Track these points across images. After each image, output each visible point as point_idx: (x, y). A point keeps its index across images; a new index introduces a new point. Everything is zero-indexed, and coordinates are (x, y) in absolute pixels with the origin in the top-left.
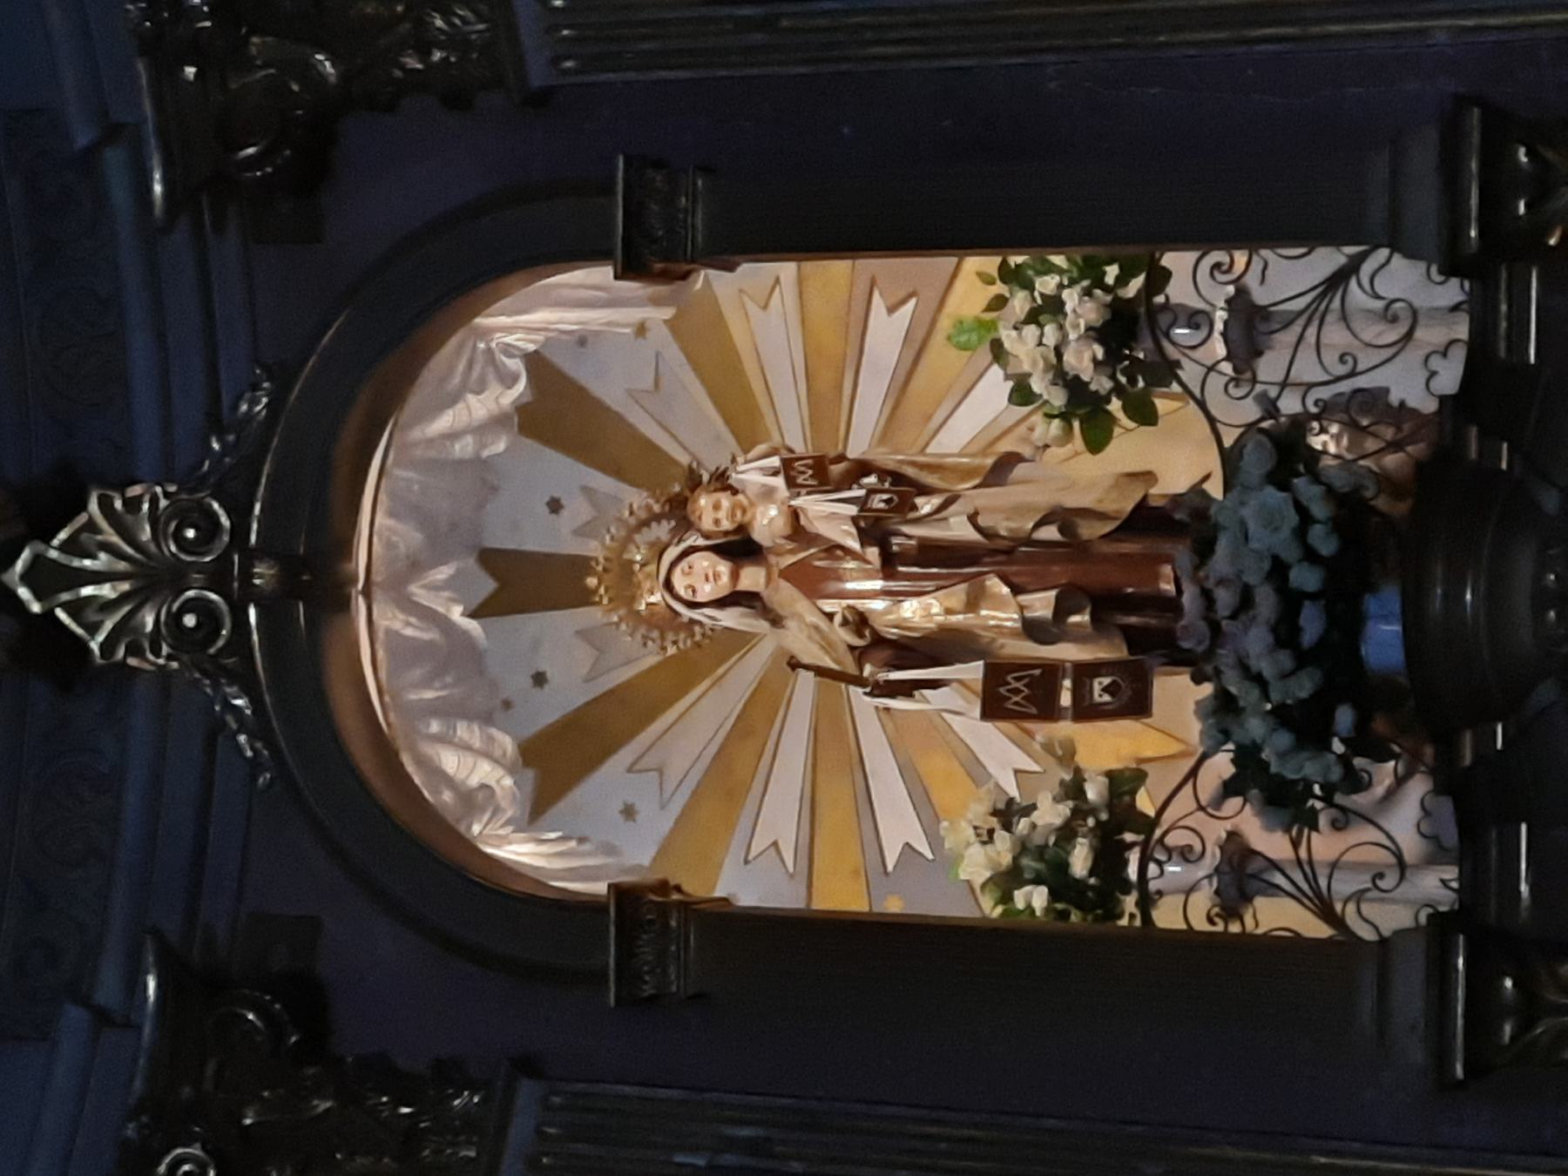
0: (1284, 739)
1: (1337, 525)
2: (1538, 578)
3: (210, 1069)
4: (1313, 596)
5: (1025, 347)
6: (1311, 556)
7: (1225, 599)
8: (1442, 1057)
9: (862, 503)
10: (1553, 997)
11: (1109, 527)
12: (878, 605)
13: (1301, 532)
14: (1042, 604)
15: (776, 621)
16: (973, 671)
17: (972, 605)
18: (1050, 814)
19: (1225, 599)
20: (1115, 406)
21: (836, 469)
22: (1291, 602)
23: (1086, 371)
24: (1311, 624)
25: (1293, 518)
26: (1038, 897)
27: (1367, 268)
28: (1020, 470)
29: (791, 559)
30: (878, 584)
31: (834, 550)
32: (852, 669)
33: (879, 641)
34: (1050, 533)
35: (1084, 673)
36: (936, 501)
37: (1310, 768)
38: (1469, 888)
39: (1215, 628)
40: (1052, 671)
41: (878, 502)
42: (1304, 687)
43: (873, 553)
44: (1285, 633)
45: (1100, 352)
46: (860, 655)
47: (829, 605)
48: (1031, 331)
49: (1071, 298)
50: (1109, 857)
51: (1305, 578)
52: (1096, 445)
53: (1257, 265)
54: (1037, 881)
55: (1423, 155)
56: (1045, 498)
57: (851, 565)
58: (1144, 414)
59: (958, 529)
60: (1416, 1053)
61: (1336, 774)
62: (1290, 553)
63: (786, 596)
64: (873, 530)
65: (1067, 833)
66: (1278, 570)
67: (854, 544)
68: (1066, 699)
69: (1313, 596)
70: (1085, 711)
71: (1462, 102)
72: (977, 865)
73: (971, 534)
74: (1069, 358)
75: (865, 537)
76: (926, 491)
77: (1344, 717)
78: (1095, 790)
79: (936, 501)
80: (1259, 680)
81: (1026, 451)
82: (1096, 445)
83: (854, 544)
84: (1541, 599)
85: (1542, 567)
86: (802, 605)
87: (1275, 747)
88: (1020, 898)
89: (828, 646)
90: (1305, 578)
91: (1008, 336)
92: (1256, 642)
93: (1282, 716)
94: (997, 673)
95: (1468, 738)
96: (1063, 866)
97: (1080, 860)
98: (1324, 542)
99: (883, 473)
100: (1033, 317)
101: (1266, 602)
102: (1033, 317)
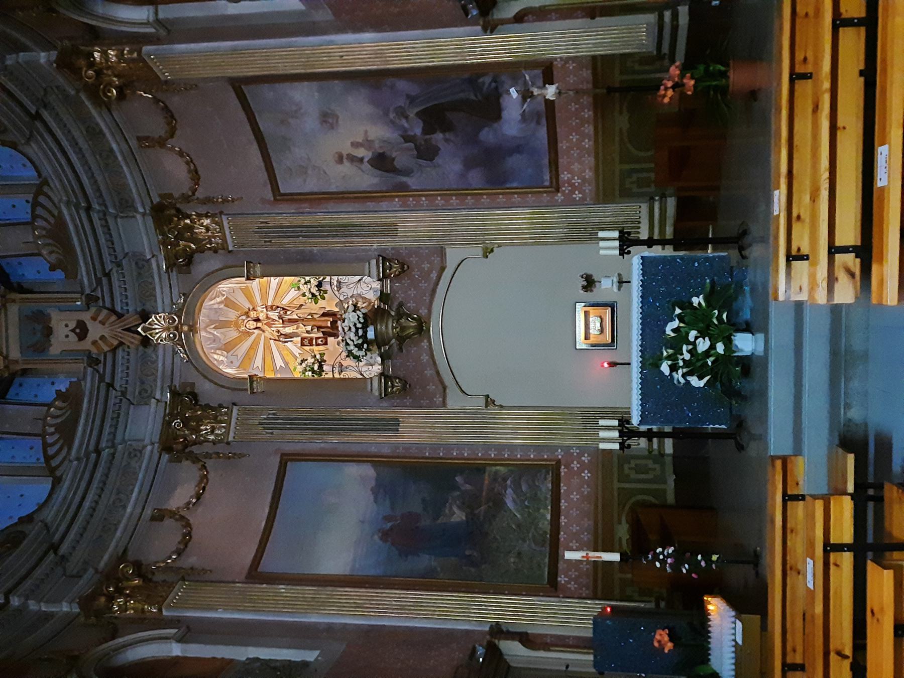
0: (357, 349)
1: (364, 318)
2: (392, 325)
3: (179, 408)
4: (361, 328)
5: (304, 289)
6: (360, 322)
7: (346, 329)
8: (381, 394)
9: (279, 313)
10: (396, 384)
11: (319, 316)
12: (281, 329)
13: (358, 319)
14: (309, 328)
15: (264, 331)
16: (299, 339)
17: (297, 329)
18: (312, 360)
19: (346, 329)
20: (319, 297)
21: (274, 307)
22: (357, 329)
23: (315, 292)
24: (360, 332)
25: (357, 317)
26: (310, 373)
27: (364, 279)
28: (303, 307)
29: (266, 322)
30: (282, 325)
31: (273, 320)
32: (277, 339)
33: (281, 334)
34: (310, 317)
35: (317, 338)
36: (290, 312)
37: (362, 353)
38: (384, 368)
39: (345, 333)
40: (311, 339)
41: (282, 313)
42: (360, 341)
43: (281, 321)
44: (356, 333)
45: (317, 289)
46: (278, 336)
47: (273, 329)
48: (305, 286)
49: (312, 281)
50: (321, 367)
51: (359, 325)
52: (316, 303)
53: (347, 278)
54: (309, 371)
55: (374, 262)
56: (309, 311)
57: (277, 322)
58: (324, 298)
59: (295, 317)
60: (377, 394)
61: (364, 354)
62: (357, 322)
63: (265, 327)
64: (280, 317)
65: (313, 363)
66: (355, 325)
67: (278, 319)
68: (314, 343)
69: (361, 328)
70: (317, 345)
71: (379, 256)
72: (300, 368)
73: (297, 317)
74: (312, 290)
75: (279, 318)
76: (288, 310)
77: (365, 346)
78: (318, 357)
79: (290, 312)
80: (353, 341)
81: (304, 304)
82: (316, 303)
83: (278, 319)
84: (393, 328)
85: (393, 323)
86: (268, 329)
87: (355, 351)
88: (307, 374)
89: (273, 335)
90: (359, 325)
91: (301, 287)
92: (352, 335)
93: (356, 346)
94: (303, 339)
95: (383, 348)
96: (313, 368)
97: (316, 367)
98: (362, 320)
99: (281, 308)
100: (306, 283)
101: (353, 329)
102: (306, 283)
